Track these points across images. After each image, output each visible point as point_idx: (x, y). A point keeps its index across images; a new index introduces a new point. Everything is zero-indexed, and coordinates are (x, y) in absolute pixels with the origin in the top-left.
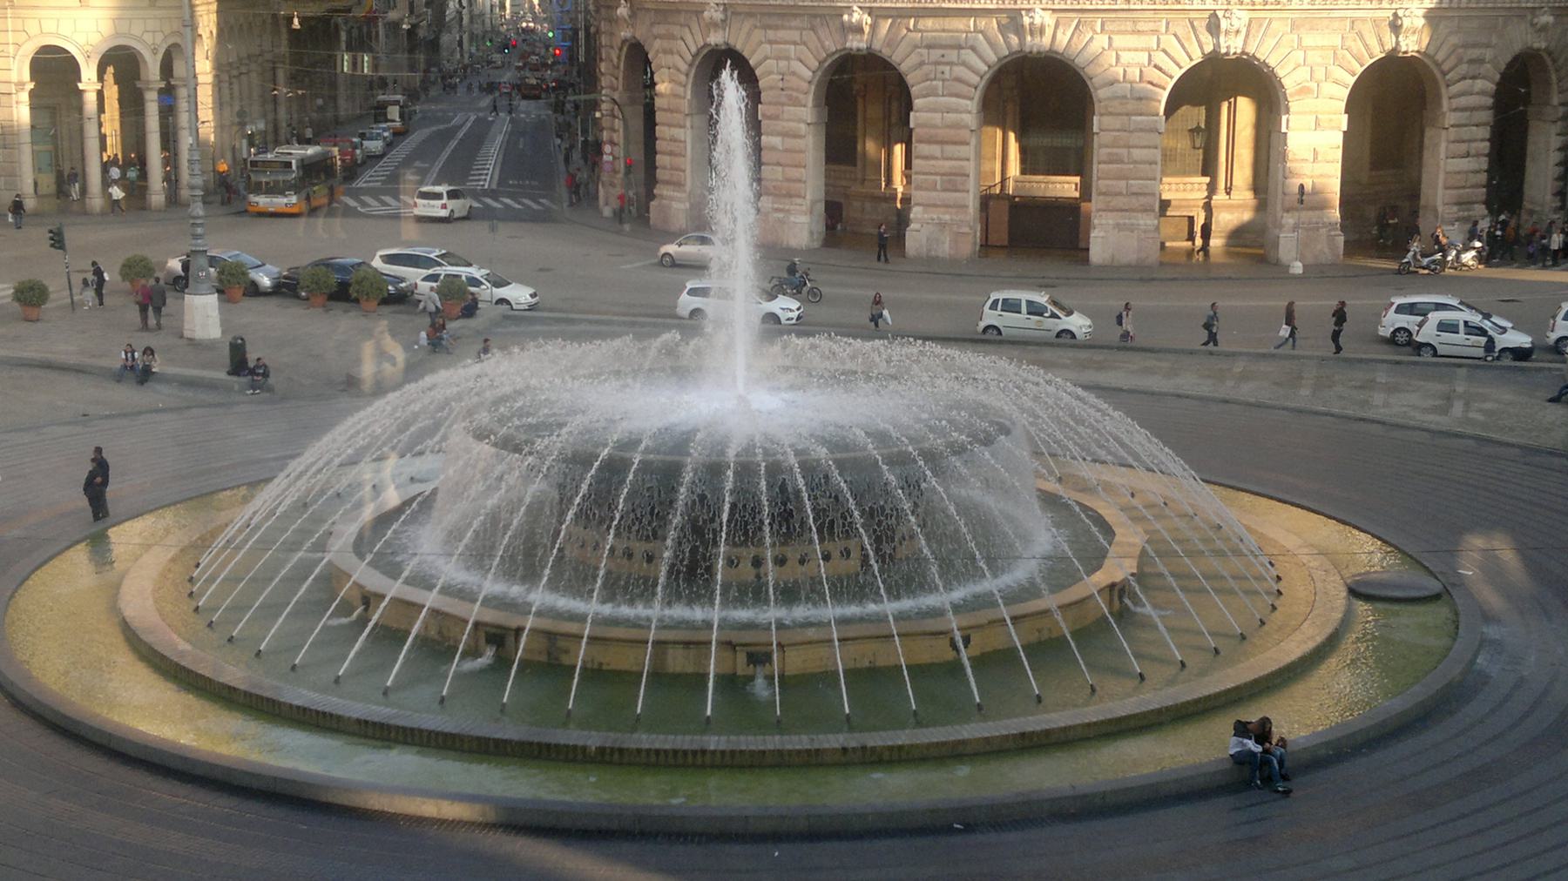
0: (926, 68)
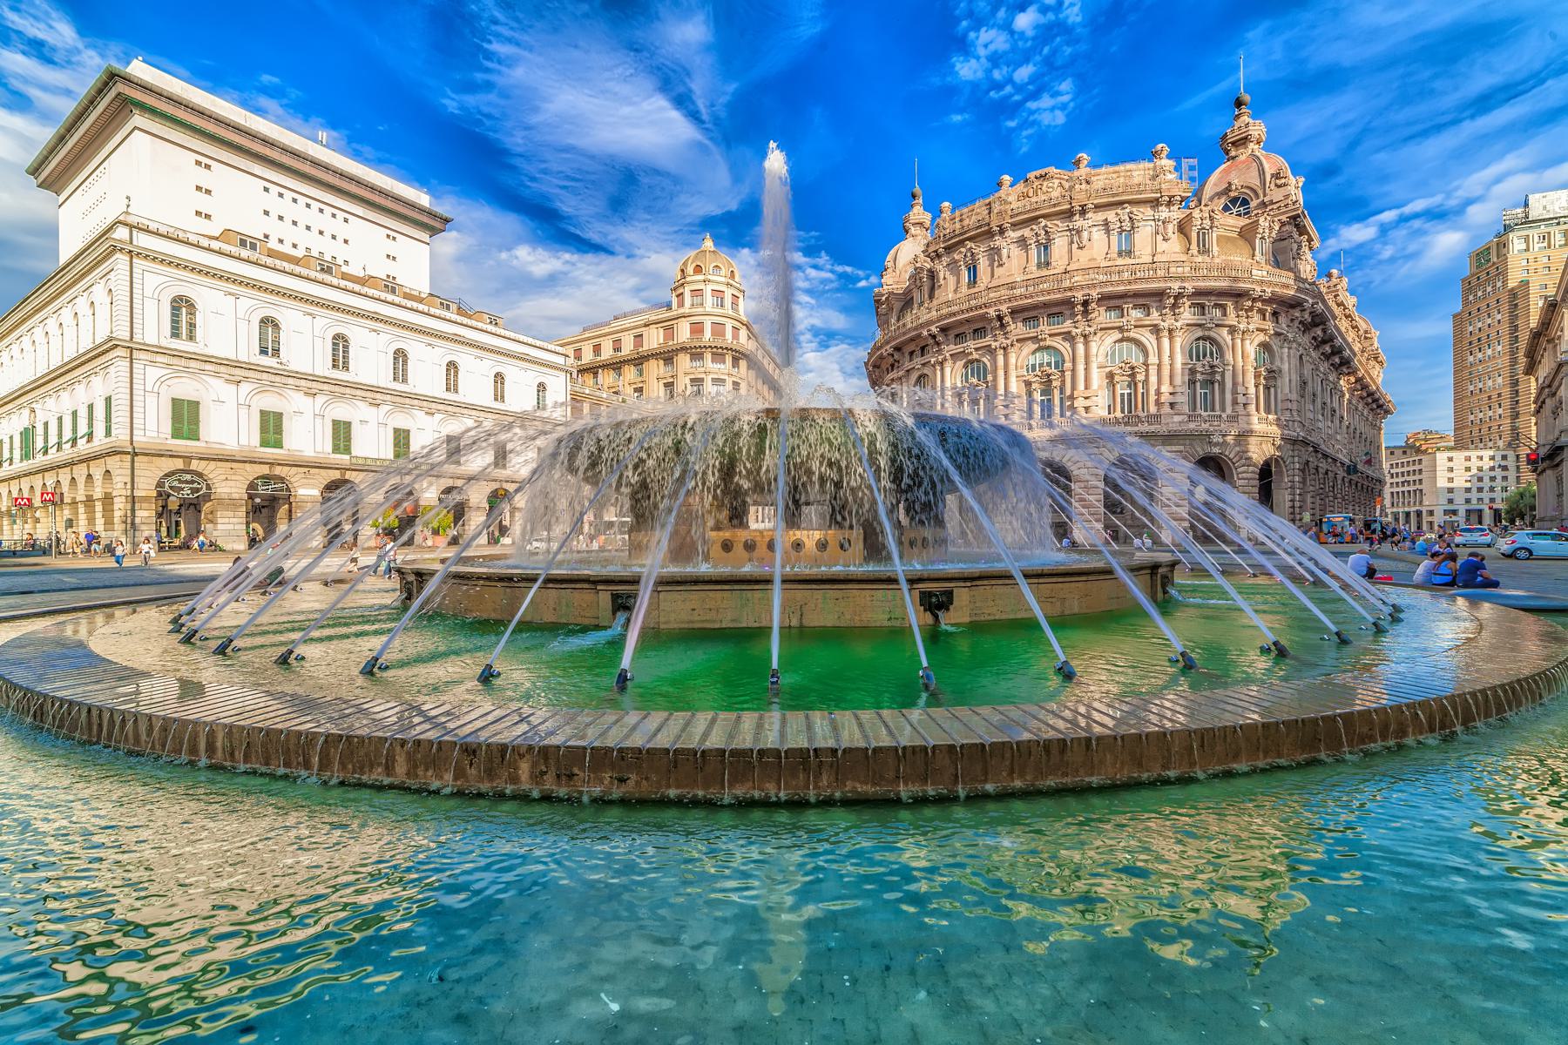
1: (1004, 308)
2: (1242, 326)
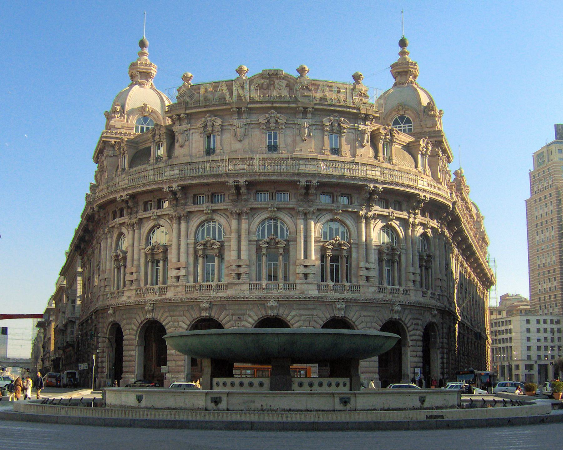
0: (231, 323)
1: (242, 181)
2: (411, 220)
